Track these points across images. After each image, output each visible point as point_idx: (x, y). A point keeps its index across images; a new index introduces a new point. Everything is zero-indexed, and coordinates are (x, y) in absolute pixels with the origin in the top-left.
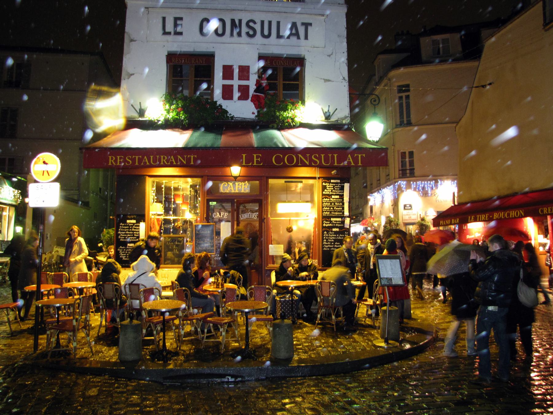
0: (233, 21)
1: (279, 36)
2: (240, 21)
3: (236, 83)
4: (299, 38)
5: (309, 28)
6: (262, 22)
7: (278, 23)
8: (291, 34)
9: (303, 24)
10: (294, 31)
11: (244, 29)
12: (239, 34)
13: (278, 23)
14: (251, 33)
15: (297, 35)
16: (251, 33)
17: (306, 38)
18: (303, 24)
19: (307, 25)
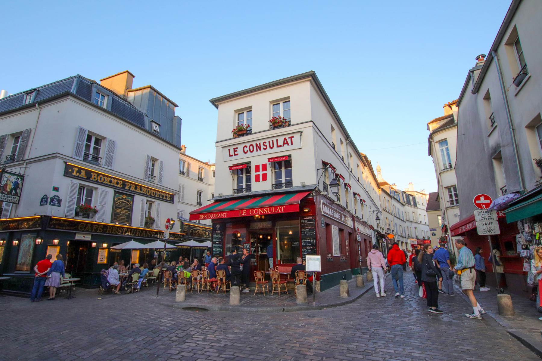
0: (257, 145)
1: (278, 146)
2: (260, 144)
3: (261, 173)
4: (288, 145)
5: (293, 139)
6: (269, 142)
7: (277, 140)
8: (284, 144)
9: (289, 138)
10: (285, 142)
11: (262, 147)
12: (260, 150)
13: (277, 140)
14: (265, 147)
15: (287, 143)
16: (265, 147)
17: (292, 144)
18: (289, 138)
19: (291, 138)
